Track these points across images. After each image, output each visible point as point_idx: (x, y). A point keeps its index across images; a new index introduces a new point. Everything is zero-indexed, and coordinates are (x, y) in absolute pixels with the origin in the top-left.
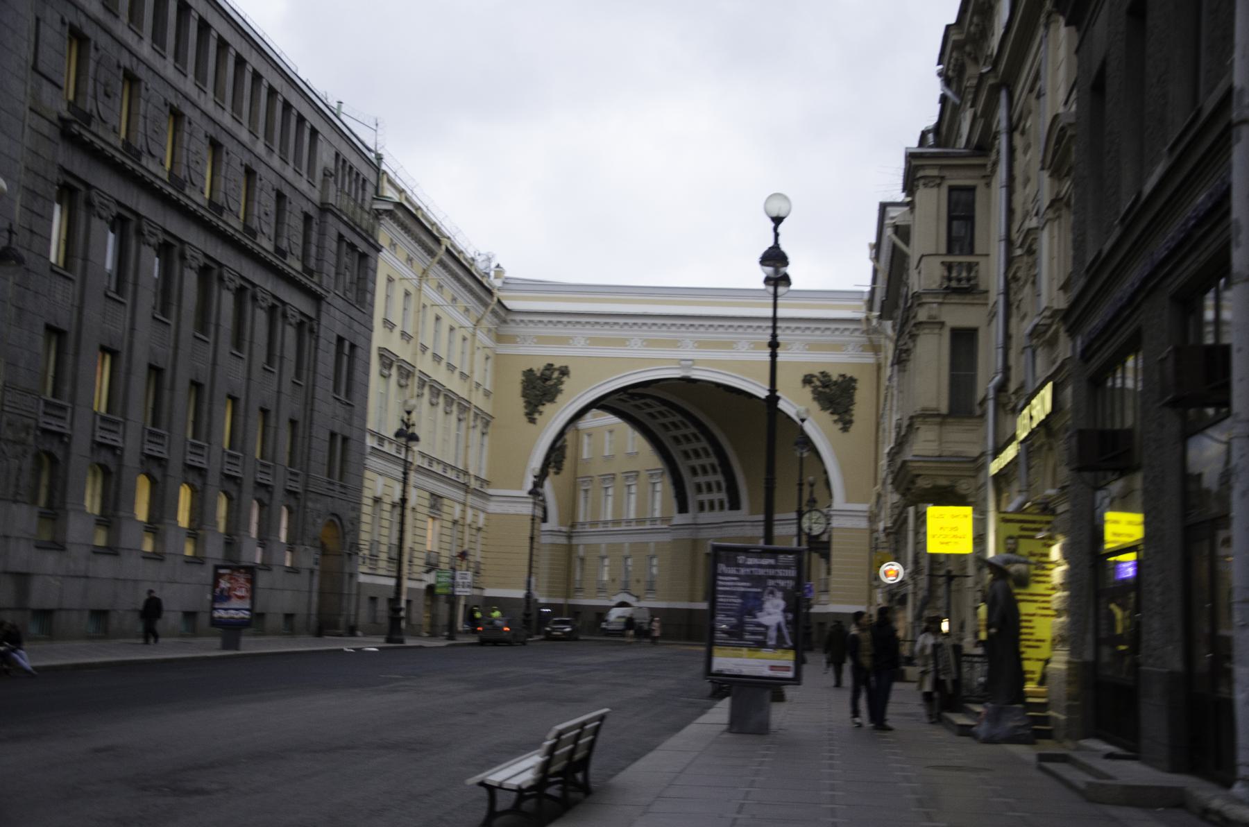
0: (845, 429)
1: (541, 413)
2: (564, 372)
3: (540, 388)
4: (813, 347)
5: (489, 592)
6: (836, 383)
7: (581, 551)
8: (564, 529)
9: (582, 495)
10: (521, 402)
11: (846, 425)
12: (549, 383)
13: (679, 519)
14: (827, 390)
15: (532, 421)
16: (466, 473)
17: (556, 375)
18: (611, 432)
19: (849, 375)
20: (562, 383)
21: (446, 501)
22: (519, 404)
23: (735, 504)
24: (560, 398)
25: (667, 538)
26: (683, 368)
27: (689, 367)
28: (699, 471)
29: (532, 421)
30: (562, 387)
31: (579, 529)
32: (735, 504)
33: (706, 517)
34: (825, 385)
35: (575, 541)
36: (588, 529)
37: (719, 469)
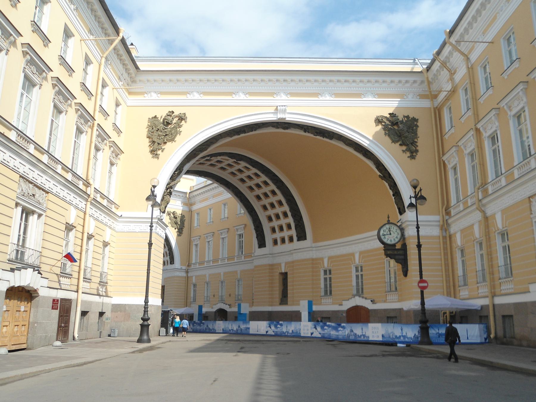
0: (412, 157)
2: (182, 118)
5: (116, 300)
6: (402, 122)
9: (194, 247)
14: (396, 127)
15: (156, 156)
16: (87, 184)
17: (175, 120)
19: (411, 116)
20: (180, 127)
23: (302, 236)
24: (178, 138)
27: (284, 111)
29: (156, 156)
30: (181, 129)
31: (192, 267)
32: (302, 236)
33: (280, 248)
36: (198, 266)
37: (289, 214)
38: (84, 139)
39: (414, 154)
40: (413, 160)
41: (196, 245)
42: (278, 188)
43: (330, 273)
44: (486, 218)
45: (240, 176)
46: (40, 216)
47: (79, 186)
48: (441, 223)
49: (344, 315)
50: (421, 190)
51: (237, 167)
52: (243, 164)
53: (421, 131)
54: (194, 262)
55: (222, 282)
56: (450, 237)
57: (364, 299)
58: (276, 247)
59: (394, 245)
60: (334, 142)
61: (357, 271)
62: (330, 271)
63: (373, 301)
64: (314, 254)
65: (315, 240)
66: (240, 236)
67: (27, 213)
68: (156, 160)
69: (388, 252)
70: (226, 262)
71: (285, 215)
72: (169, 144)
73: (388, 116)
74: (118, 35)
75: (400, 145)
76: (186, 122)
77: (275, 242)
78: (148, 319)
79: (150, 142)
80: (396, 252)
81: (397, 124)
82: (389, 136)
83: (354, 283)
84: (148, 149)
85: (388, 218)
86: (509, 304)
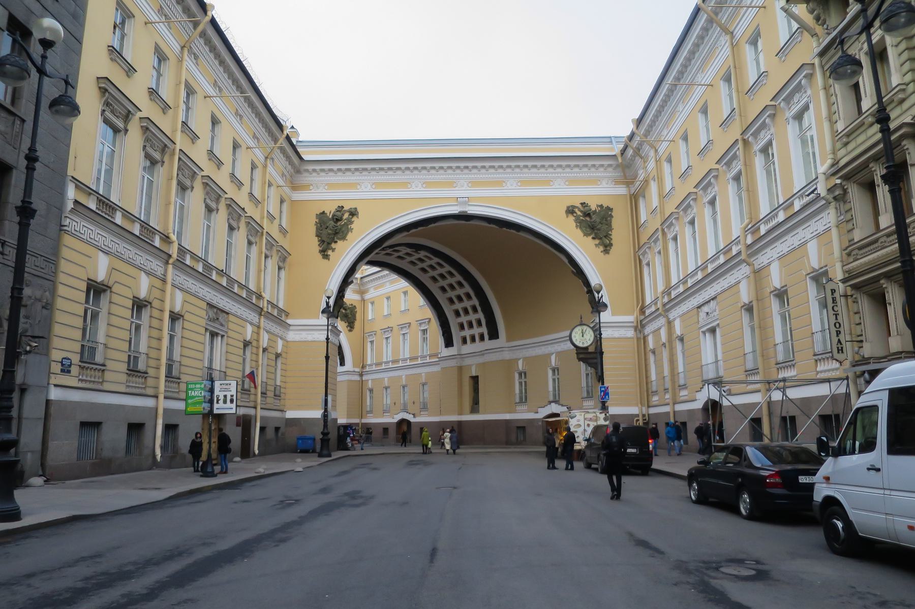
1: (333, 250)
2: (353, 213)
3: (332, 229)
4: (572, 182)
5: (290, 414)
7: (370, 385)
8: (357, 370)
10: (315, 241)
11: (607, 248)
12: (339, 223)
14: (588, 219)
16: (260, 297)
17: (346, 216)
18: (388, 298)
19: (605, 206)
20: (352, 223)
21: (231, 318)
22: (314, 244)
23: (494, 335)
24: (350, 236)
27: (465, 203)
28: (461, 313)
30: (353, 226)
31: (367, 369)
32: (494, 335)
33: (469, 348)
35: (364, 378)
36: (374, 368)
37: (479, 309)
38: (254, 248)
41: (372, 342)
42: (465, 279)
46: (222, 336)
47: (252, 300)
51: (417, 256)
52: (422, 254)
54: (369, 362)
58: (465, 347)
59: (587, 348)
60: (522, 234)
62: (525, 374)
64: (507, 355)
65: (509, 339)
67: (213, 335)
68: (326, 261)
69: (581, 356)
71: (475, 310)
72: (340, 243)
73: (580, 206)
74: (282, 132)
75: (593, 238)
77: (464, 341)
78: (328, 434)
80: (588, 356)
81: (589, 215)
83: (551, 388)
84: (318, 249)
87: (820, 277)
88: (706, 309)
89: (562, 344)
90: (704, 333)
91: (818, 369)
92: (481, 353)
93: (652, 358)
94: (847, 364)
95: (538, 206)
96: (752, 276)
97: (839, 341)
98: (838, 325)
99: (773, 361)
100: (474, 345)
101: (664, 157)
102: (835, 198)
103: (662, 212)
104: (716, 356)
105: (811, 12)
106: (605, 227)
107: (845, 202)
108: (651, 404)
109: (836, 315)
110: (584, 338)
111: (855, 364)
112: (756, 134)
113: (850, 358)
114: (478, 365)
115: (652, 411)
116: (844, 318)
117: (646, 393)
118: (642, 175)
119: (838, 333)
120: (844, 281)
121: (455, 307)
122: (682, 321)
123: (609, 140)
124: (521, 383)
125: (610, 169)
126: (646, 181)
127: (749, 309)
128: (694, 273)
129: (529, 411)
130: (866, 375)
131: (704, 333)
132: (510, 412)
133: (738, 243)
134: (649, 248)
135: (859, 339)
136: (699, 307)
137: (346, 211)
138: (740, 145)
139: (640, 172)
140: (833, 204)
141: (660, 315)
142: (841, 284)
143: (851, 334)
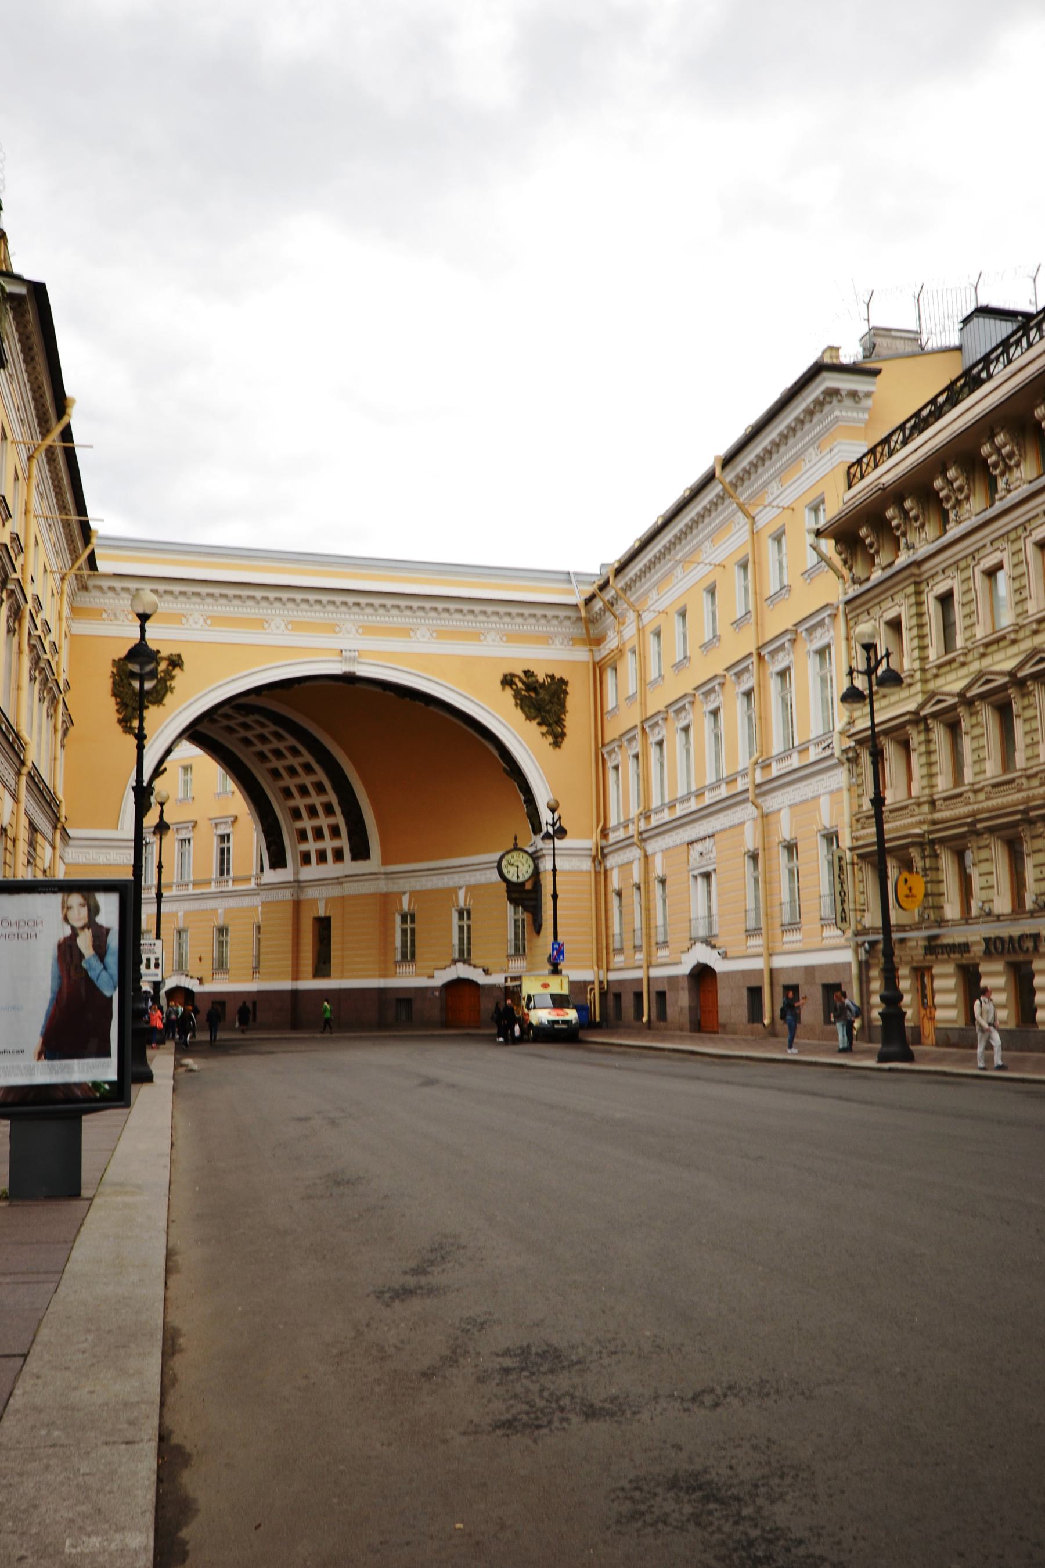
0: (557, 744)
4: (512, 638)
6: (543, 685)
10: (111, 703)
11: (558, 739)
13: (271, 876)
19: (557, 676)
20: (172, 678)
23: (361, 852)
24: (169, 699)
25: (255, 901)
26: (347, 660)
27: (353, 660)
30: (174, 683)
32: (361, 852)
33: (312, 871)
34: (529, 687)
39: (560, 739)
40: (557, 749)
42: (318, 762)
43: (413, 921)
44: (646, 857)
45: (260, 747)
48: (594, 852)
49: (437, 994)
50: (560, 818)
53: (571, 702)
55: (179, 932)
56: (606, 871)
57: (472, 968)
59: (523, 884)
61: (461, 918)
62: (413, 917)
63: (486, 972)
64: (382, 886)
65: (385, 862)
66: (224, 838)
69: (514, 895)
70: (191, 890)
73: (522, 675)
75: (539, 724)
76: (182, 670)
79: (117, 704)
82: (522, 708)
84: (115, 716)
85: (516, 839)
86: (663, 978)
87: (831, 838)
88: (699, 847)
89: (477, 873)
90: (695, 877)
91: (824, 935)
92: (338, 881)
93: (614, 901)
94: (849, 933)
95: (462, 672)
96: (759, 820)
97: (843, 910)
98: (843, 894)
99: (777, 922)
100: (323, 867)
101: (649, 629)
102: (848, 760)
103: (643, 705)
104: (709, 908)
105: (840, 554)
106: (556, 708)
107: (857, 765)
108: (611, 966)
109: (842, 883)
110: (519, 869)
111: (857, 934)
112: (773, 653)
113: (853, 927)
114: (328, 901)
115: (613, 976)
116: (849, 888)
117: (604, 951)
118: (612, 643)
119: (843, 902)
120: (851, 849)
121: (292, 803)
122: (663, 858)
123: (567, 577)
124: (404, 932)
125: (567, 623)
126: (620, 651)
127: (754, 857)
128: (685, 799)
129: (417, 975)
130: (866, 945)
131: (695, 877)
132: (384, 976)
133: (745, 775)
134: (620, 747)
135: (862, 908)
136: (690, 843)
137: (162, 659)
138: (754, 659)
139: (611, 634)
140: (846, 765)
141: (633, 844)
142: (848, 852)
143: (855, 902)
